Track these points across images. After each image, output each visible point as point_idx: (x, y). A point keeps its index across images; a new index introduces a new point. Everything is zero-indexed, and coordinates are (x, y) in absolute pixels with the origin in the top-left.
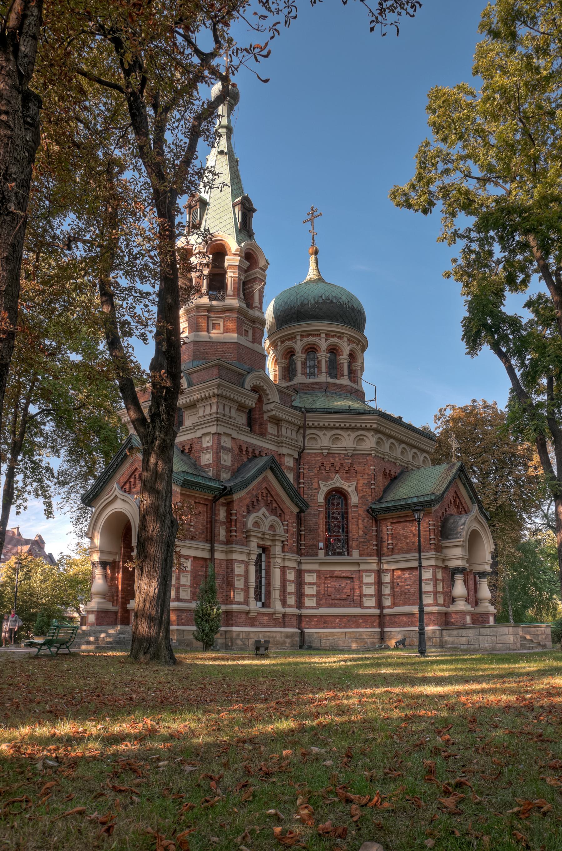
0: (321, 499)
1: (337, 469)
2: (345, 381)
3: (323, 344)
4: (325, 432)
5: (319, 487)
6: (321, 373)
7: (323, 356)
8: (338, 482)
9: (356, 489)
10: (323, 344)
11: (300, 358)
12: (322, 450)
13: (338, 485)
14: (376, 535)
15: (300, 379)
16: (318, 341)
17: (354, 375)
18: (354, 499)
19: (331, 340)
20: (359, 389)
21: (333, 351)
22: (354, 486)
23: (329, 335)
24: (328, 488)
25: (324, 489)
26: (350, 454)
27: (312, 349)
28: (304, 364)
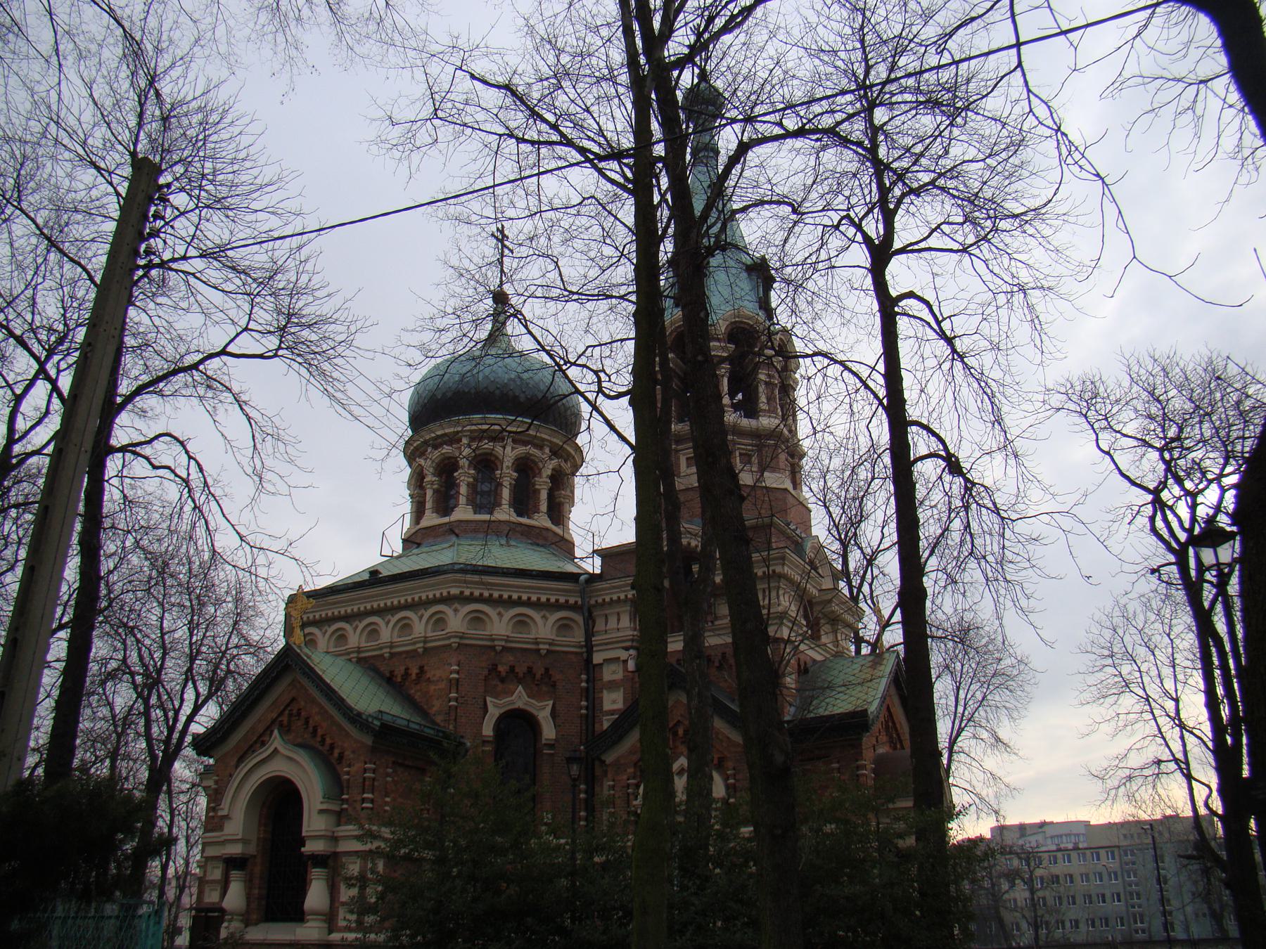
0: (488, 730)
1: (521, 675)
2: (541, 520)
3: (509, 454)
4: (500, 609)
5: (485, 710)
6: (500, 505)
7: (507, 476)
8: (519, 698)
9: (554, 714)
10: (509, 454)
11: (464, 477)
12: (493, 640)
13: (519, 704)
14: (586, 800)
15: (463, 512)
16: (499, 450)
17: (558, 512)
18: (549, 732)
19: (522, 450)
20: (566, 536)
21: (525, 468)
22: (549, 709)
23: (519, 439)
24: (502, 711)
25: (494, 712)
26: (543, 652)
27: (485, 464)
28: (472, 487)
